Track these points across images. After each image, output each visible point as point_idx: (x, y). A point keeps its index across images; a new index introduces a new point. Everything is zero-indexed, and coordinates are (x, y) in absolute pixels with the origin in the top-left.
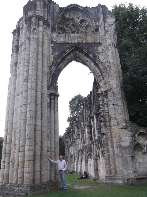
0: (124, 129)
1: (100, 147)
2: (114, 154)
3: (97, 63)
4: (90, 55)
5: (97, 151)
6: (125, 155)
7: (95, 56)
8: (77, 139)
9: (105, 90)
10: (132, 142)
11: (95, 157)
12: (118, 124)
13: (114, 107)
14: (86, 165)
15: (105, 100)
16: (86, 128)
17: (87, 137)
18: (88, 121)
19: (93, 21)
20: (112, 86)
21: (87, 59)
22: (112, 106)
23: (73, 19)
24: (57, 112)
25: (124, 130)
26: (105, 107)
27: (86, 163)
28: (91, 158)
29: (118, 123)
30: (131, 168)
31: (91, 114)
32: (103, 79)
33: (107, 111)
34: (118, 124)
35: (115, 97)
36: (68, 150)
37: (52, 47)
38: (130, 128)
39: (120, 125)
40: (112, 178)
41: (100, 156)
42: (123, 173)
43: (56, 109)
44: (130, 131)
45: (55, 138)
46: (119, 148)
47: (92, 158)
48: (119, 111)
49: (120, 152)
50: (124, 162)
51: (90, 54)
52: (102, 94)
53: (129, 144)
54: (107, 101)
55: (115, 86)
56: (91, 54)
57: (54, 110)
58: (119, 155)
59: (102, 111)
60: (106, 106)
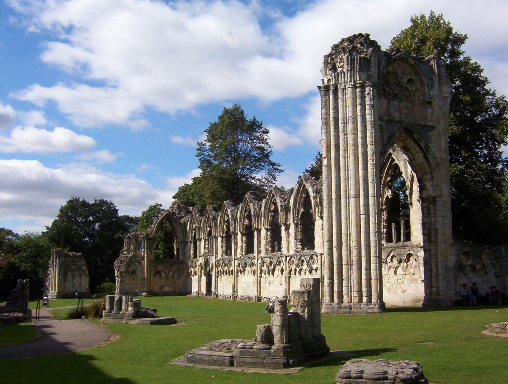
3: (428, 156)
4: (421, 144)
7: (427, 147)
9: (433, 194)
15: (432, 208)
19: (426, 86)
21: (416, 146)
23: (396, 72)
26: (432, 217)
34: (446, 241)
36: (185, 246)
37: (380, 125)
46: (444, 268)
51: (421, 141)
54: (435, 210)
56: (423, 142)
60: (432, 216)
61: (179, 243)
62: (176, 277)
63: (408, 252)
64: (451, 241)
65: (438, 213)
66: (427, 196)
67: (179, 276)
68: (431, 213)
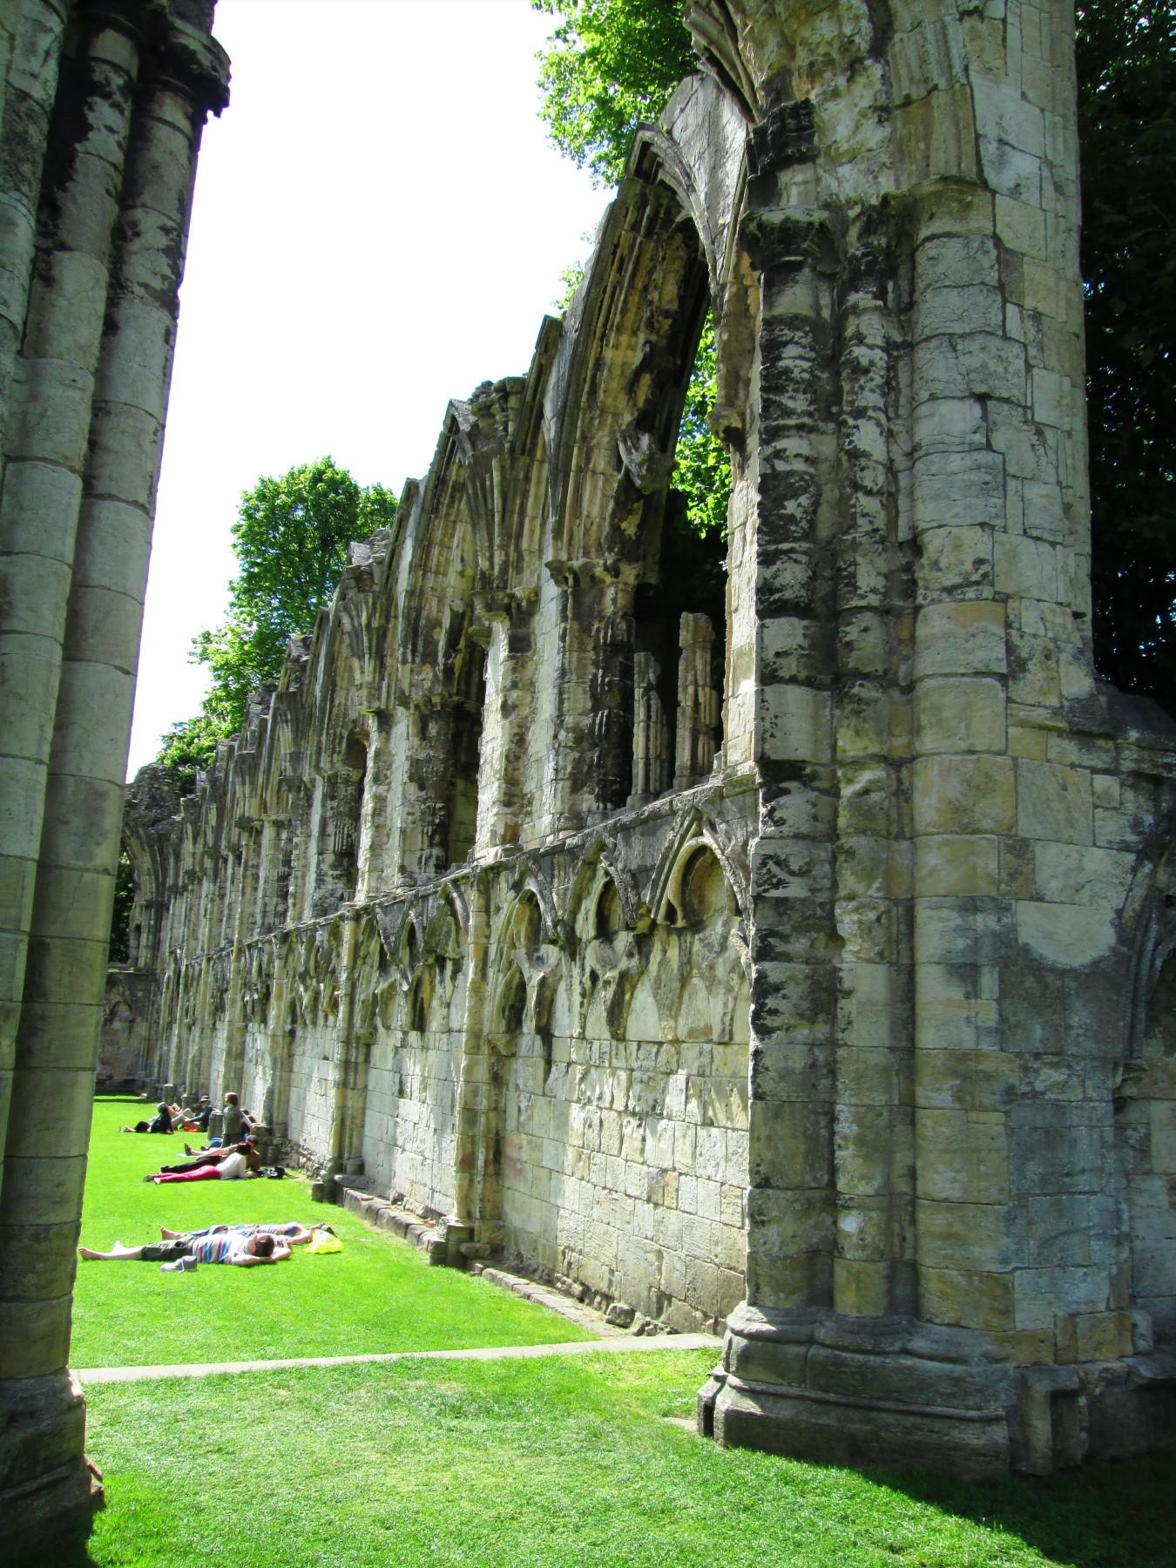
0: (1083, 736)
1: (586, 927)
2: (906, 1050)
5: (534, 977)
6: (1049, 1076)
8: (268, 833)
10: (1142, 921)
11: (493, 1023)
12: (1016, 667)
13: (988, 425)
14: (343, 1085)
16: (404, 724)
17: (397, 818)
18: (429, 657)
20: (989, 150)
22: (960, 417)
24: (158, 315)
25: (1070, 750)
26: (860, 413)
27: (347, 1066)
28: (419, 1021)
29: (1010, 649)
30: (1095, 1245)
31: (515, 564)
32: (879, 48)
33: (873, 477)
34: (1016, 667)
35: (1011, 309)
36: (159, 919)
38: (1139, 745)
39: (1035, 673)
40: (838, 1363)
41: (566, 1022)
42: (1007, 1312)
43: (143, 267)
44: (1137, 779)
45: (62, 725)
46: (989, 981)
47: (435, 1024)
48: (1034, 492)
49: (1004, 1030)
50: (1034, 1168)
52: (825, 236)
53: (1105, 938)
55: (1023, 166)
57: (117, 286)
58: (989, 1077)
59: (799, 466)
60: (871, 398)
61: (141, 906)
62: (117, 1025)
63: (690, 844)
64: (1078, 681)
65: (936, 366)
66: (820, 216)
67: (132, 1021)
68: (860, 370)
